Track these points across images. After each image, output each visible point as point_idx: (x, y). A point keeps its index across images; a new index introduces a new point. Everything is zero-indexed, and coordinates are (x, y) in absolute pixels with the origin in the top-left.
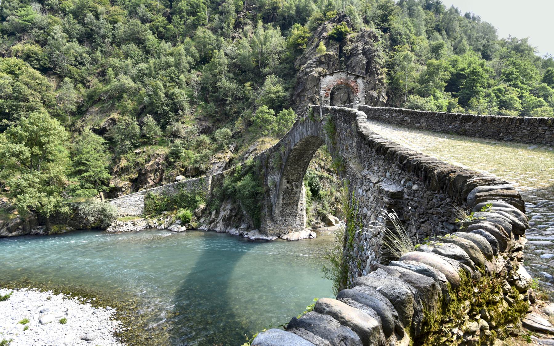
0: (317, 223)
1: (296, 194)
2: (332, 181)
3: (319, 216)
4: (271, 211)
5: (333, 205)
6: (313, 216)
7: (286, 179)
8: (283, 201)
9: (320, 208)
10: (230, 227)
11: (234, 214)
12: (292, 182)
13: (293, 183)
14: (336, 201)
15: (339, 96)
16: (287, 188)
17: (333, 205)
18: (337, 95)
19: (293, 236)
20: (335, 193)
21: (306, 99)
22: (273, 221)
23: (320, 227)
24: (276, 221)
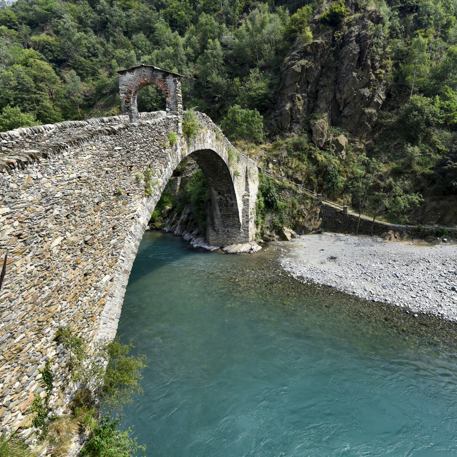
0: (270, 236)
1: (232, 206)
2: (296, 192)
3: (274, 228)
4: (213, 220)
5: (294, 218)
6: (267, 228)
7: (216, 190)
8: (220, 212)
9: (276, 220)
10: (185, 231)
11: (191, 219)
12: (224, 194)
13: (226, 195)
14: (298, 214)
15: (324, 95)
16: (221, 199)
17: (294, 218)
18: (322, 93)
19: (233, 248)
20: (298, 206)
21: (286, 98)
22: (215, 230)
23: (273, 240)
24: (218, 231)
